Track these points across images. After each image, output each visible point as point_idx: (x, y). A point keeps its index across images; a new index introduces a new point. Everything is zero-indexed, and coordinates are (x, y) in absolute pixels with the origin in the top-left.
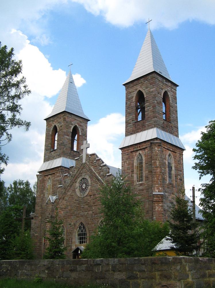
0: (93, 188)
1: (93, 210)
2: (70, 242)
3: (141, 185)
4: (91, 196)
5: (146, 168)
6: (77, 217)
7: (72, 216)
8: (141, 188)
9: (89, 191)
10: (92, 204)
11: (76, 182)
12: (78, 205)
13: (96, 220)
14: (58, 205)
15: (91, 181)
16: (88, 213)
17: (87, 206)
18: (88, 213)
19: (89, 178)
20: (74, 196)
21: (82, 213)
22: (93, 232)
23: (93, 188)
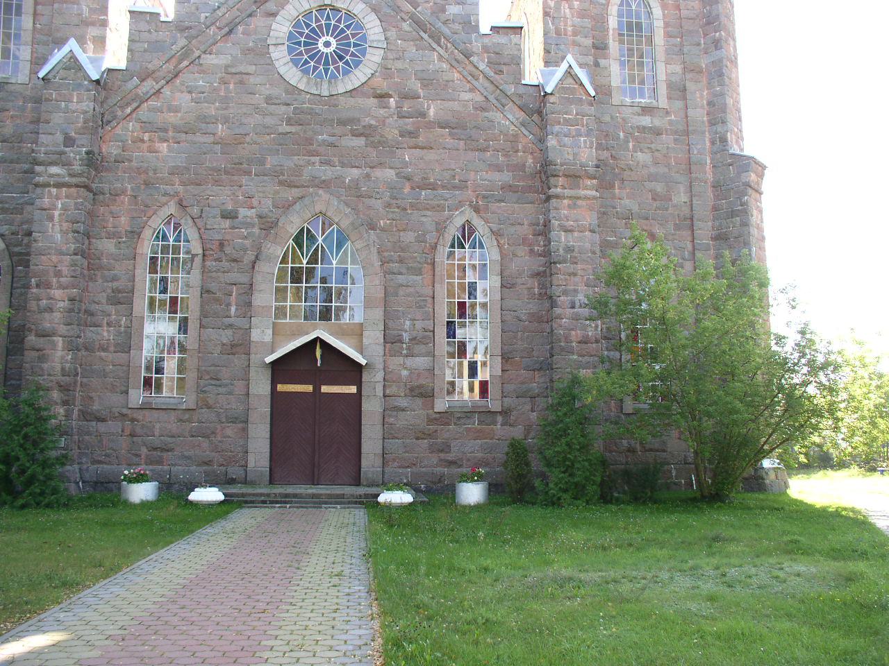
0: (399, 65)
1: (406, 165)
2: (229, 305)
3: (647, 110)
4: (383, 96)
5: (667, 52)
6: (281, 183)
7: (248, 173)
8: (646, 121)
9: (369, 72)
10: (392, 133)
11: (274, 15)
12: (288, 129)
13: (429, 213)
14: (128, 104)
15: (385, 30)
16: (368, 176)
17: (361, 141)
18: (368, 176)
19: (373, 16)
20: (252, 80)
21: (327, 173)
22: (408, 269)
23: (399, 65)
